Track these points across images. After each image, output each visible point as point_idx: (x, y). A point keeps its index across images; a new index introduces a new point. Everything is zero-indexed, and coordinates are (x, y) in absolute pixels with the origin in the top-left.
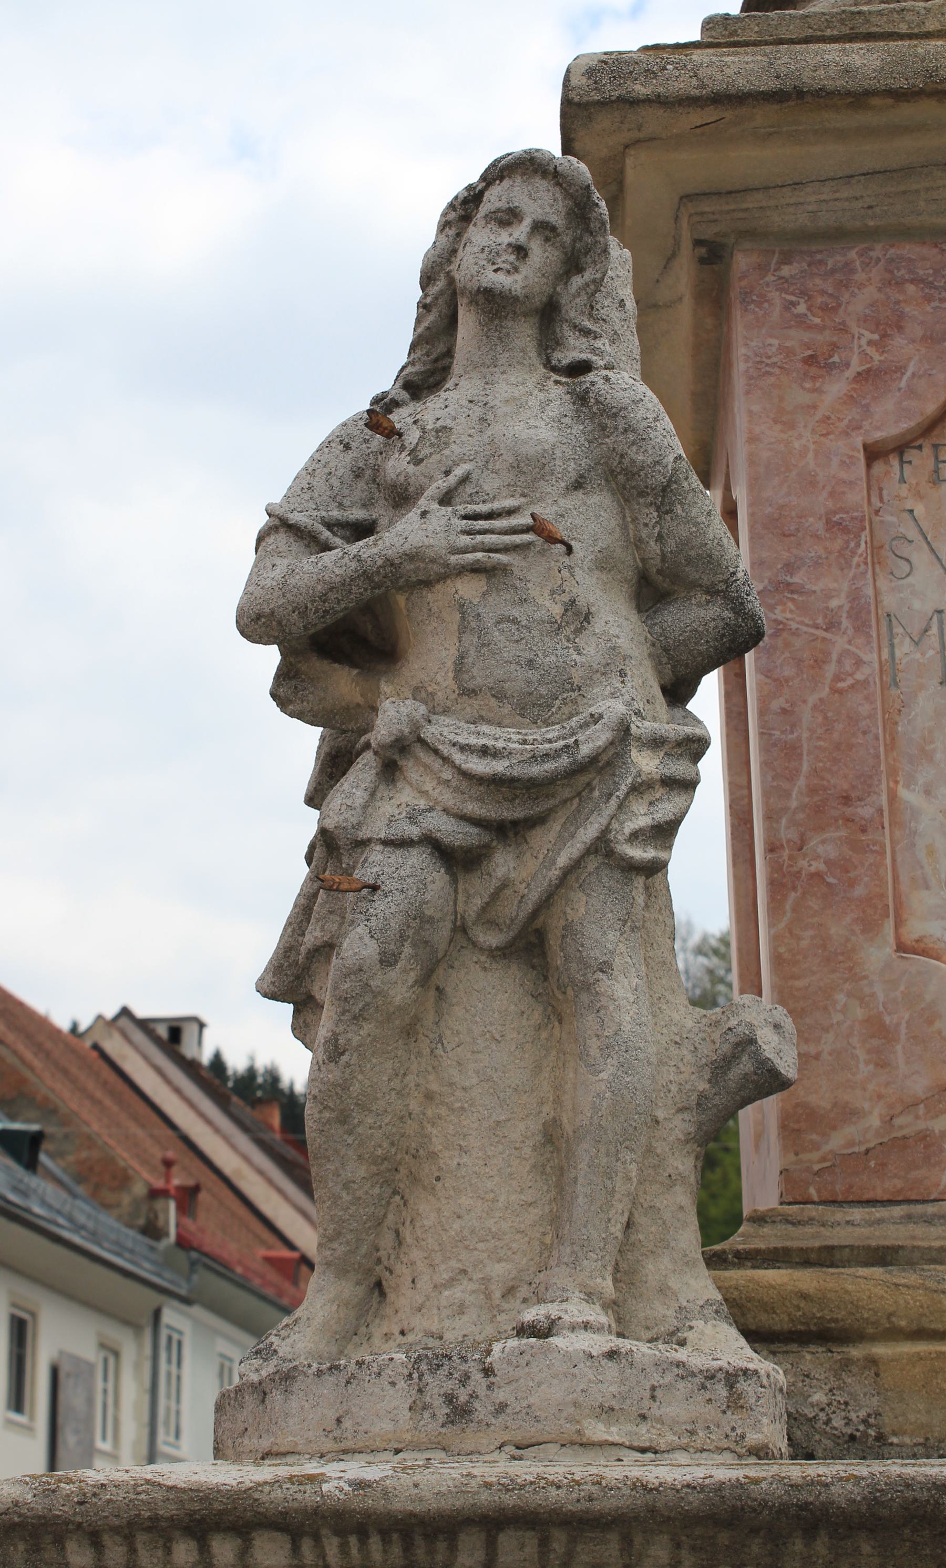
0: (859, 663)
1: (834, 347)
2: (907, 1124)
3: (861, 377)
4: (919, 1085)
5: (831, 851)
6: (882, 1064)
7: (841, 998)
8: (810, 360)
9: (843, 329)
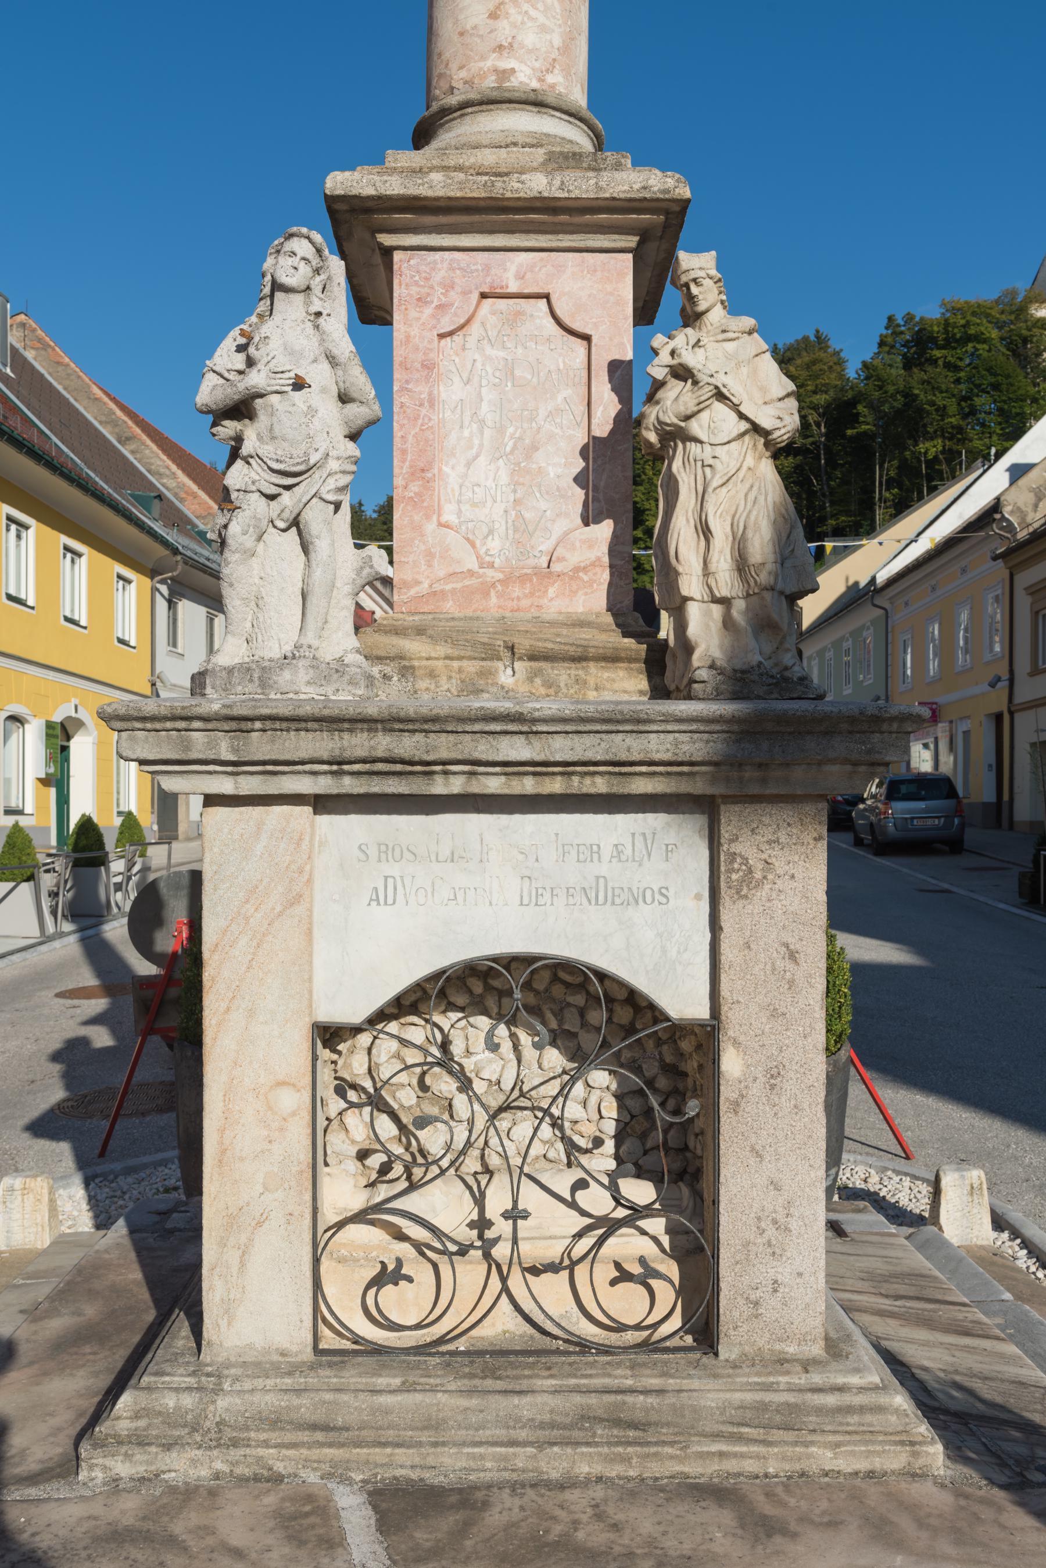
0: (430, 419)
1: (428, 294)
2: (437, 587)
4: (442, 574)
5: (416, 489)
6: (430, 566)
8: (419, 300)
9: (432, 287)
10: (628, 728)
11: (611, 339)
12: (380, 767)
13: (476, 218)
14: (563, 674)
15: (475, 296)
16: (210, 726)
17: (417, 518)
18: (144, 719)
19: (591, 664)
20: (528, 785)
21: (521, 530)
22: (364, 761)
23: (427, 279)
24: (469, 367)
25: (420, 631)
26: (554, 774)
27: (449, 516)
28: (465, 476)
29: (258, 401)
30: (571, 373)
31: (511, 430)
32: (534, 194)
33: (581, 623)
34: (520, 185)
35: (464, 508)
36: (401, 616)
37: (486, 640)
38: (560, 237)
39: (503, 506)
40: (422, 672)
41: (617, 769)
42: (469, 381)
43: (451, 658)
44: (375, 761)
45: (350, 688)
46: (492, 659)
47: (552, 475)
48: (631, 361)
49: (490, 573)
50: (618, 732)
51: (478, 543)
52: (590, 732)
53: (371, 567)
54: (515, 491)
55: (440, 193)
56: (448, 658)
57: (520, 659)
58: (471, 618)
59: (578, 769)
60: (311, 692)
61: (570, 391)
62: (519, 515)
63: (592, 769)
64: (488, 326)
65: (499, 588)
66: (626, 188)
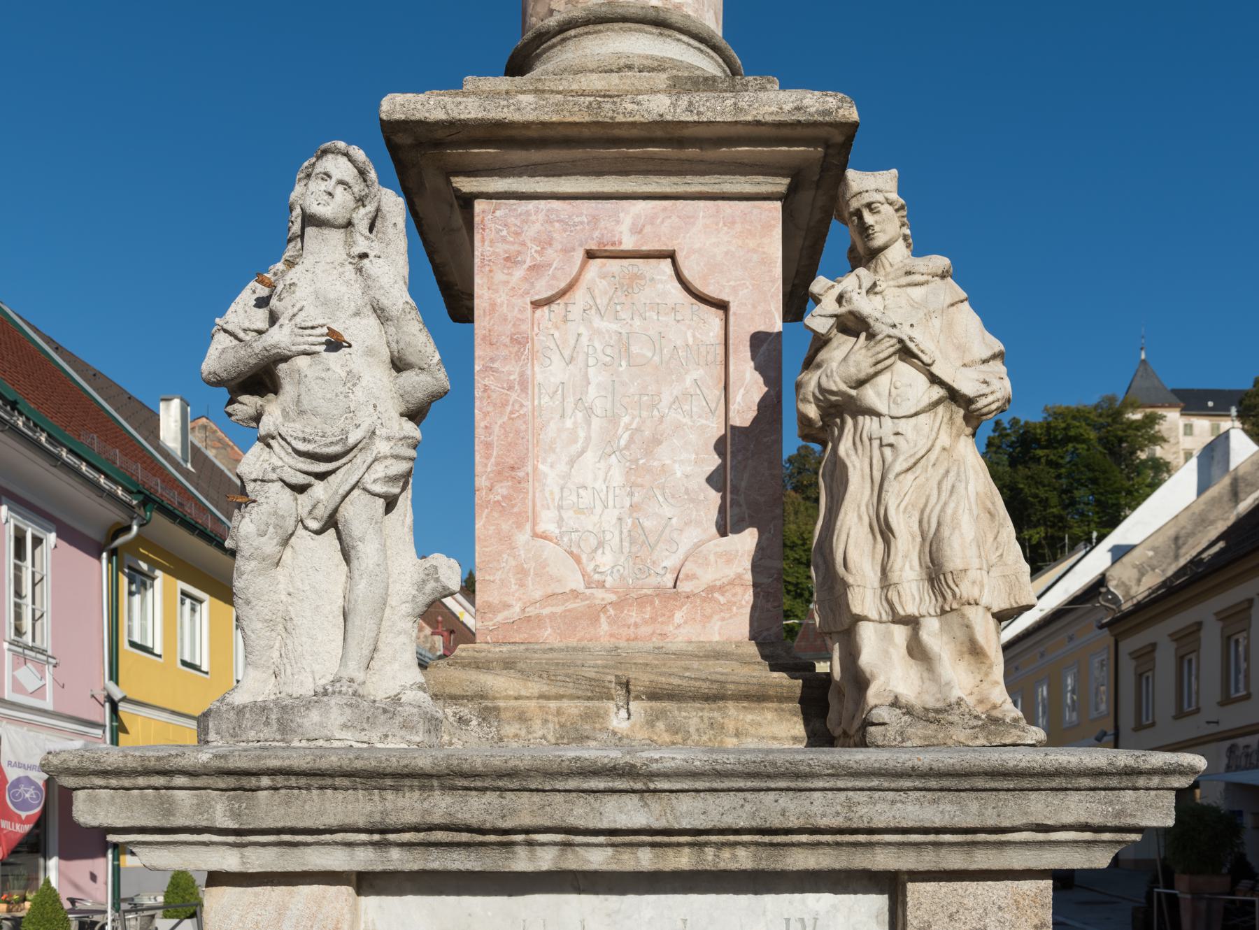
0: (522, 406)
1: (519, 253)
2: (532, 611)
3: (532, 268)
4: (538, 595)
5: (505, 491)
6: (522, 585)
7: (505, 556)
8: (507, 259)
9: (523, 244)
10: (782, 784)
11: (754, 307)
12: (439, 836)
13: (578, 153)
14: (693, 717)
15: (579, 255)
16: (199, 782)
17: (505, 527)
18: (105, 773)
19: (730, 704)
20: (645, 860)
21: (639, 542)
22: (416, 829)
23: (517, 234)
24: (572, 342)
25: (508, 664)
26: (679, 845)
27: (547, 523)
28: (567, 476)
29: (282, 367)
30: (703, 349)
31: (626, 419)
32: (653, 117)
33: (717, 655)
34: (636, 107)
35: (565, 515)
36: (485, 646)
37: (592, 675)
38: (689, 179)
39: (616, 512)
40: (509, 714)
41: (767, 839)
42: (572, 359)
43: (548, 698)
44: (431, 828)
45: (403, 733)
46: (600, 698)
47: (679, 474)
48: (779, 334)
49: (599, 594)
50: (769, 789)
51: (584, 558)
52: (729, 790)
53: (437, 580)
54: (631, 494)
55: (531, 116)
56: (542, 697)
57: (637, 698)
58: (574, 649)
59: (713, 838)
60: (350, 738)
61: (701, 372)
62: (637, 523)
63: (732, 838)
64: (597, 293)
65: (611, 612)
66: (774, 109)
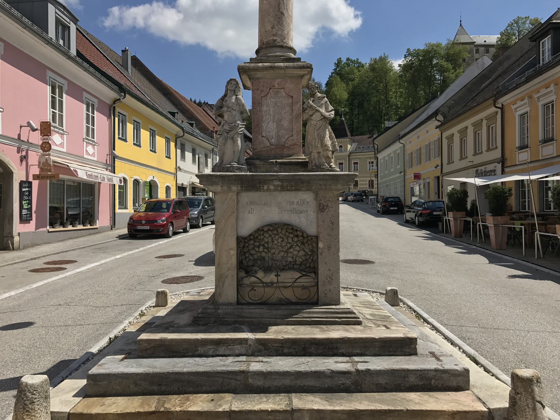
21: (279, 137)
28: (267, 126)
